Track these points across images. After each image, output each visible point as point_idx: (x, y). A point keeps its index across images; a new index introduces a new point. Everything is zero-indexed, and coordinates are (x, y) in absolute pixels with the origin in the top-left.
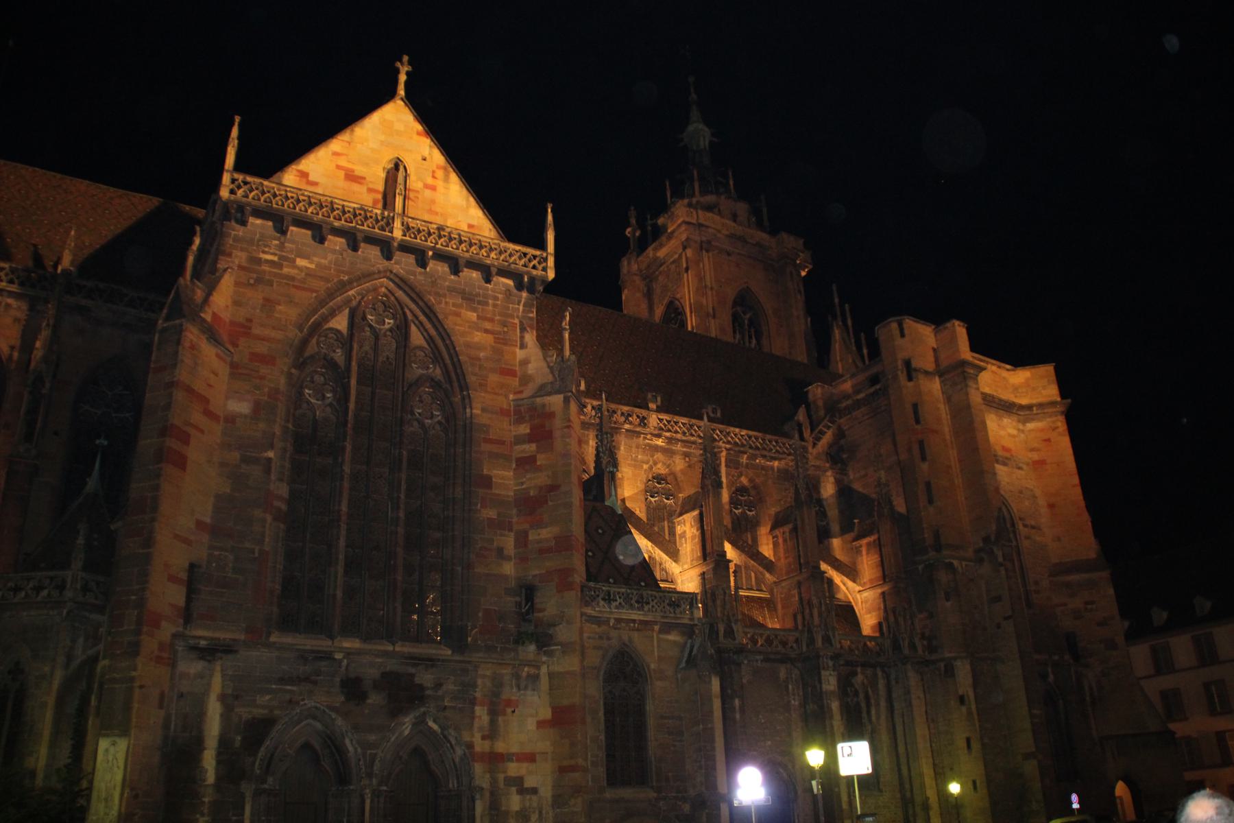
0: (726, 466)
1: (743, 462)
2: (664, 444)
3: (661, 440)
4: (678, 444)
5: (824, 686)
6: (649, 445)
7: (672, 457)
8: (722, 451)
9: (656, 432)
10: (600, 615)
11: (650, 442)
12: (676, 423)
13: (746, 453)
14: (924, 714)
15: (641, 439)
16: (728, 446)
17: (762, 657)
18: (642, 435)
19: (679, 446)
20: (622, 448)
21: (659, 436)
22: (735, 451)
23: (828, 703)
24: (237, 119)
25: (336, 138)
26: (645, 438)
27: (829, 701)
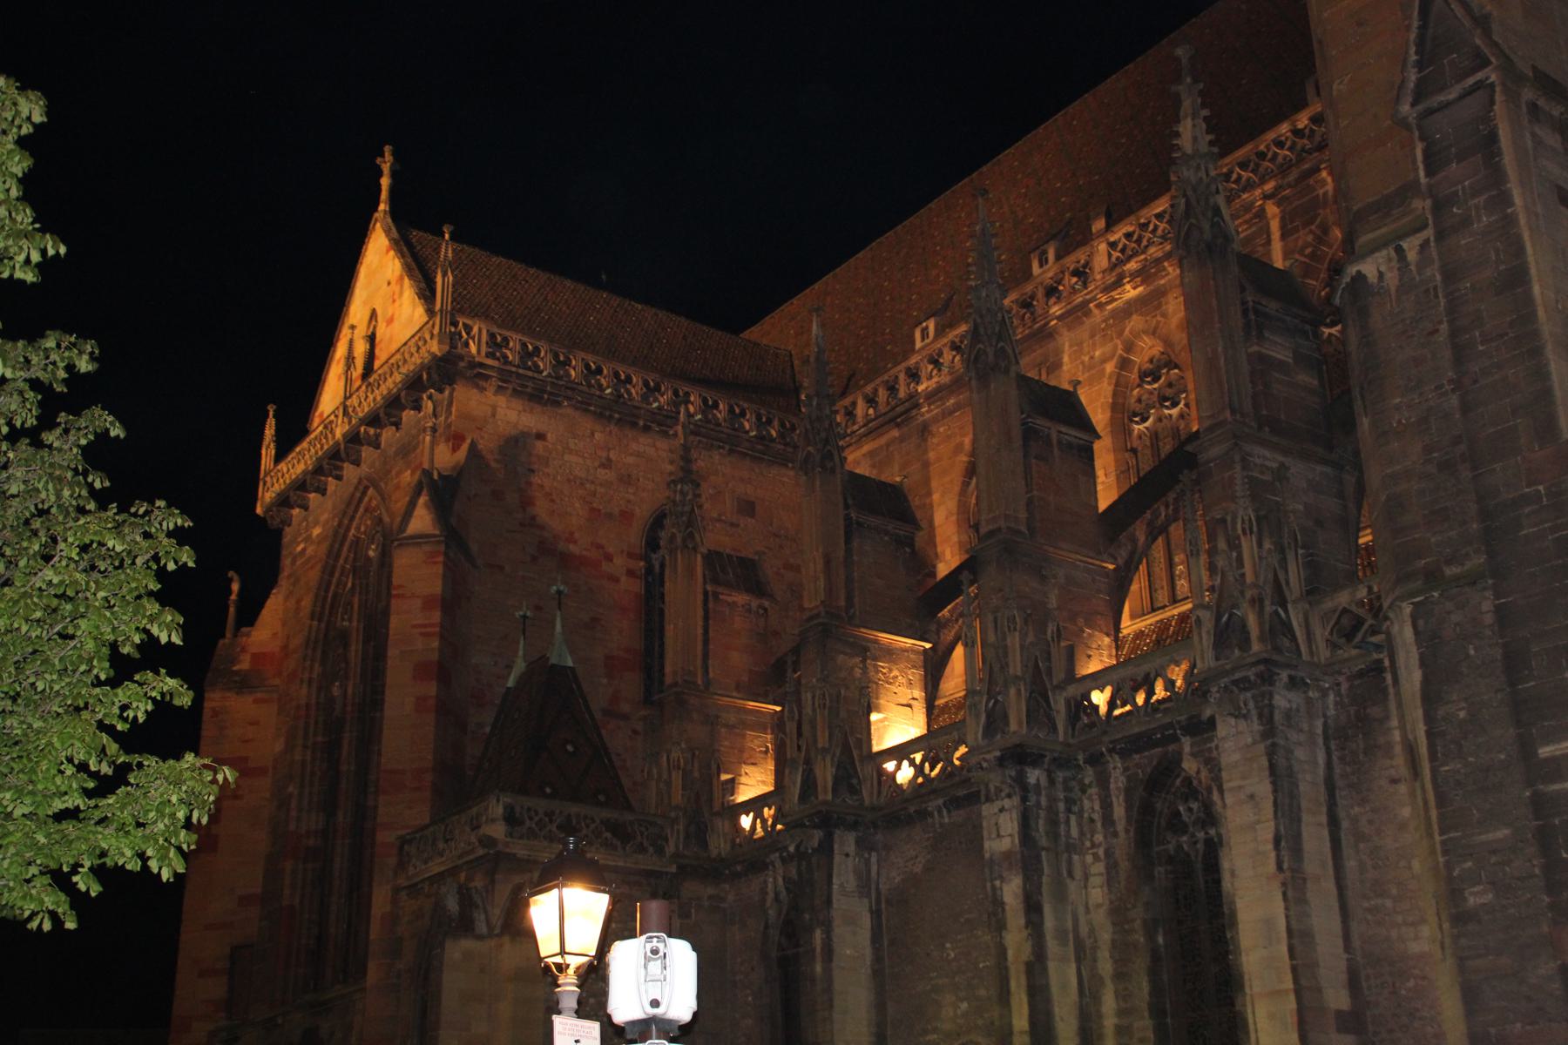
0: (1283, 237)
1: (1325, 194)
2: (1141, 289)
3: (1128, 287)
4: (1164, 269)
5: (987, 845)
6: (1115, 314)
7: (1159, 306)
8: (1262, 210)
9: (1111, 279)
10: (819, 789)
11: (1114, 304)
12: (1144, 226)
13: (1318, 170)
14: (1270, 846)
15: (1096, 311)
16: (1269, 186)
17: (940, 802)
18: (1091, 305)
19: (1170, 269)
20: (1066, 359)
21: (1118, 283)
22: (1289, 186)
23: (994, 887)
24: (271, 409)
25: (337, 341)
26: (1100, 306)
27: (997, 883)
